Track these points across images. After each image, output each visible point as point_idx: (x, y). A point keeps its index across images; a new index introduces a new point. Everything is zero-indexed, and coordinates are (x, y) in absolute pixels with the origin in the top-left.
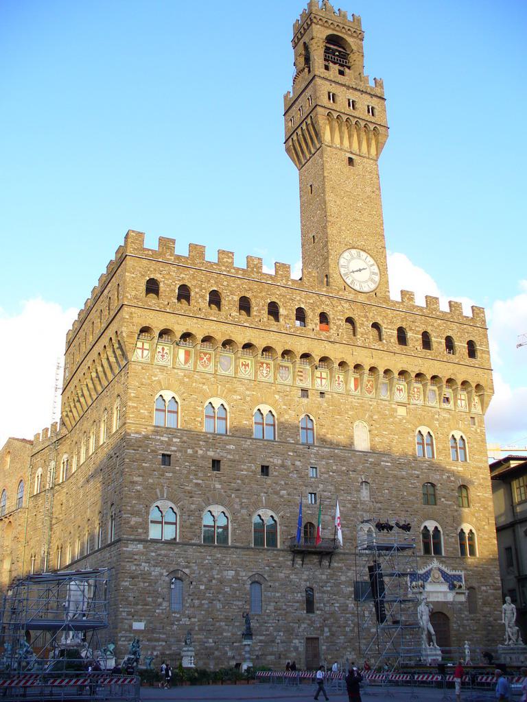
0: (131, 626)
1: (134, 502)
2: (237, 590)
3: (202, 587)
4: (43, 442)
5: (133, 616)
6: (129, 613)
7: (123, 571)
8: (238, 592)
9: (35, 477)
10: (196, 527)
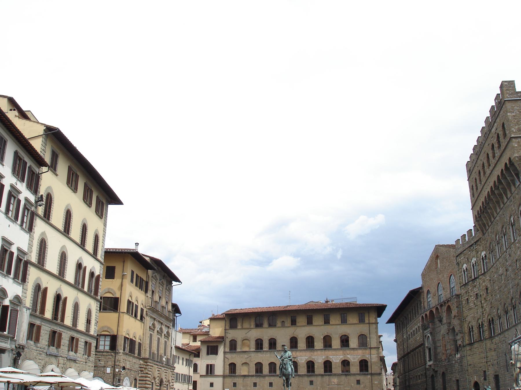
4: (463, 245)
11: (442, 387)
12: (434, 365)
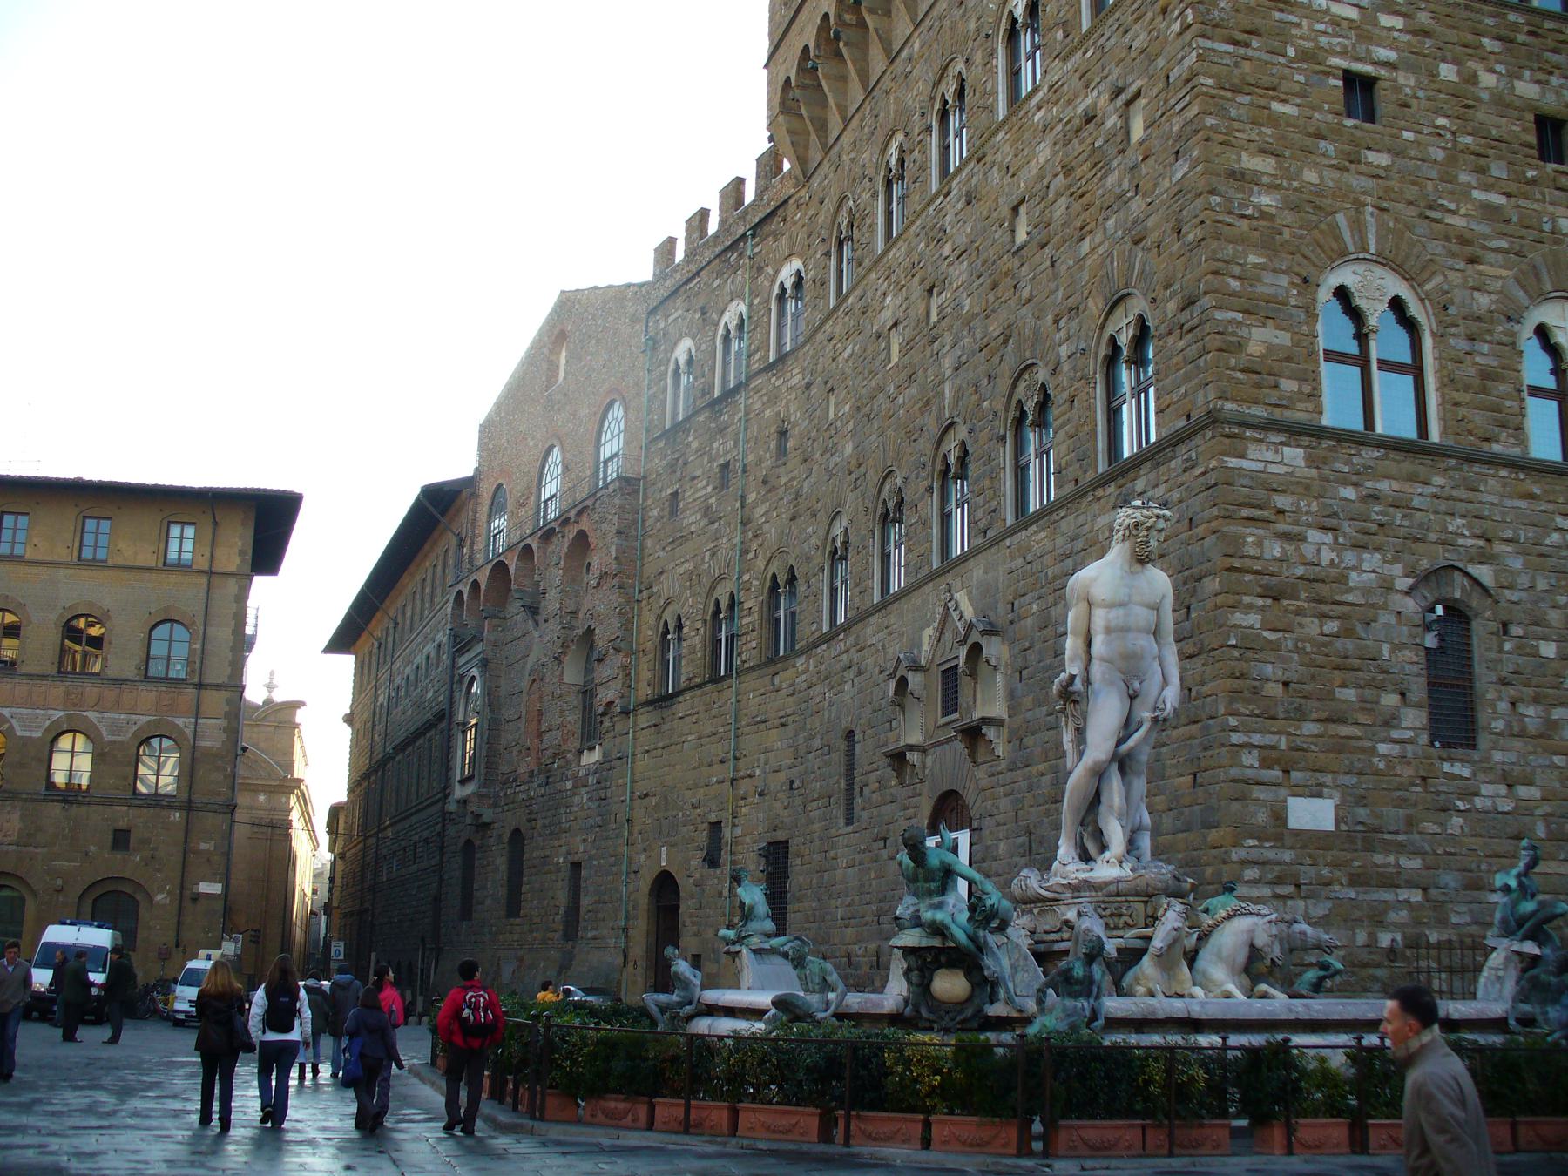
0: (1280, 817)
1: (1253, 259)
3: (1549, 650)
4: (691, 254)
5: (1287, 772)
6: (1269, 758)
10: (1502, 388)
12: (481, 796)
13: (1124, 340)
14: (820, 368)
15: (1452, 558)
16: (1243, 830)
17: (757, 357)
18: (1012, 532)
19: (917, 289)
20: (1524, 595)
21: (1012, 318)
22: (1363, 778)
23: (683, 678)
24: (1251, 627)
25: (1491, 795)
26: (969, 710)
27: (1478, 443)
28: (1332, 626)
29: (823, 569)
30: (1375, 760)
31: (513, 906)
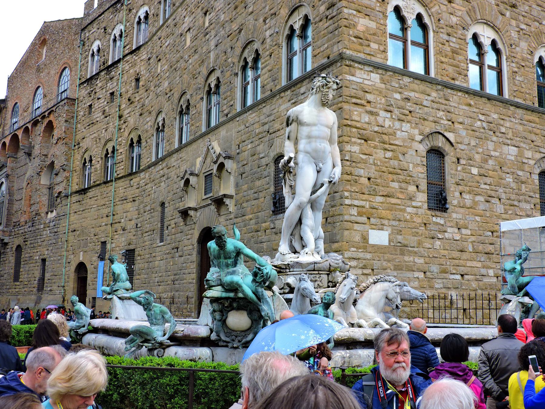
0: (365, 239)
2: (523, 183)
3: (475, 171)
5: (369, 218)
7: (349, 123)
8: (523, 186)
9: (87, 56)
10: (461, 58)
11: (12, 271)
13: (297, 27)
14: (155, 51)
15: (439, 129)
16: (351, 244)
17: (127, 47)
18: (239, 114)
19: (199, 12)
20: (466, 147)
21: (243, 21)
22: (401, 223)
23: (92, 182)
24: (355, 152)
25: (452, 233)
26: (217, 192)
27: (450, 80)
28: (389, 154)
29: (153, 135)
30: (406, 215)
31: (16, 277)
